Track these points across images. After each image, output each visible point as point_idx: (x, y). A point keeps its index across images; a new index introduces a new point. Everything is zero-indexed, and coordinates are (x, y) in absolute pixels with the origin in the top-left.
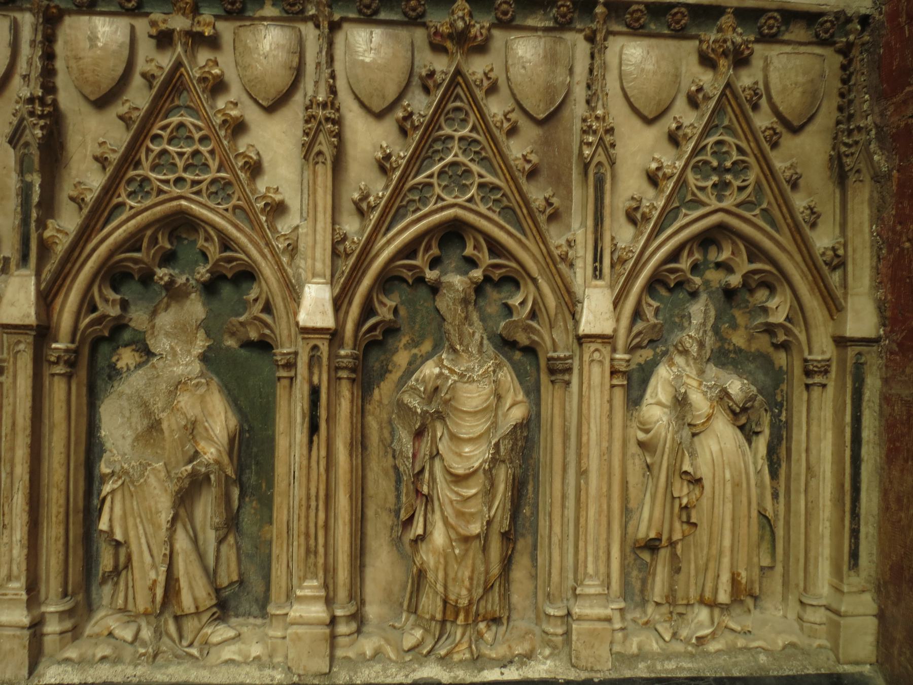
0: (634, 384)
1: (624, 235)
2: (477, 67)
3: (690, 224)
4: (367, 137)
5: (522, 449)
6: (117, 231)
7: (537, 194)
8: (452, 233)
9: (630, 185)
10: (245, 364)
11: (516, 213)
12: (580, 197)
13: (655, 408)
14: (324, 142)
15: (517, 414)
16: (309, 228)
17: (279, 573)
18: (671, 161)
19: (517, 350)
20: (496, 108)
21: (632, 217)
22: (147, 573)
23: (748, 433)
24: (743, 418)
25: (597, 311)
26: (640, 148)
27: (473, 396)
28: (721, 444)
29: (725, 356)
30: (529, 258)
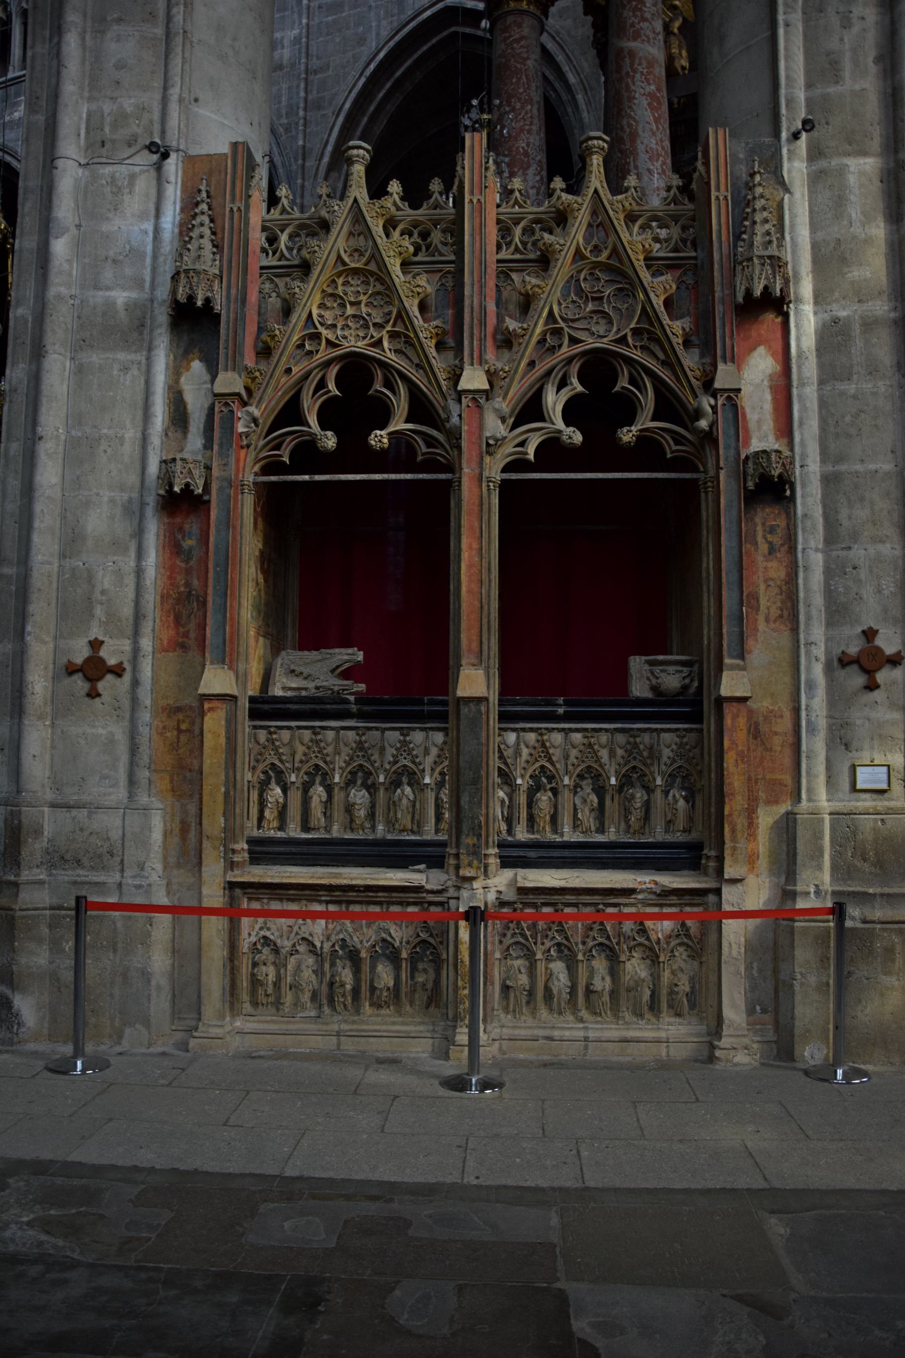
0: (666, 793)
1: (663, 767)
2: (638, 740)
3: (676, 765)
4: (620, 752)
5: (647, 805)
6: (580, 769)
7: (649, 761)
8: (634, 767)
9: (664, 759)
10: (600, 791)
11: (645, 764)
12: (656, 762)
14: (612, 754)
16: (611, 769)
18: (671, 754)
20: (641, 747)
21: (665, 764)
24: (686, 799)
25: (659, 781)
26: (666, 753)
27: (638, 795)
28: (681, 803)
29: (683, 788)
30: (647, 772)
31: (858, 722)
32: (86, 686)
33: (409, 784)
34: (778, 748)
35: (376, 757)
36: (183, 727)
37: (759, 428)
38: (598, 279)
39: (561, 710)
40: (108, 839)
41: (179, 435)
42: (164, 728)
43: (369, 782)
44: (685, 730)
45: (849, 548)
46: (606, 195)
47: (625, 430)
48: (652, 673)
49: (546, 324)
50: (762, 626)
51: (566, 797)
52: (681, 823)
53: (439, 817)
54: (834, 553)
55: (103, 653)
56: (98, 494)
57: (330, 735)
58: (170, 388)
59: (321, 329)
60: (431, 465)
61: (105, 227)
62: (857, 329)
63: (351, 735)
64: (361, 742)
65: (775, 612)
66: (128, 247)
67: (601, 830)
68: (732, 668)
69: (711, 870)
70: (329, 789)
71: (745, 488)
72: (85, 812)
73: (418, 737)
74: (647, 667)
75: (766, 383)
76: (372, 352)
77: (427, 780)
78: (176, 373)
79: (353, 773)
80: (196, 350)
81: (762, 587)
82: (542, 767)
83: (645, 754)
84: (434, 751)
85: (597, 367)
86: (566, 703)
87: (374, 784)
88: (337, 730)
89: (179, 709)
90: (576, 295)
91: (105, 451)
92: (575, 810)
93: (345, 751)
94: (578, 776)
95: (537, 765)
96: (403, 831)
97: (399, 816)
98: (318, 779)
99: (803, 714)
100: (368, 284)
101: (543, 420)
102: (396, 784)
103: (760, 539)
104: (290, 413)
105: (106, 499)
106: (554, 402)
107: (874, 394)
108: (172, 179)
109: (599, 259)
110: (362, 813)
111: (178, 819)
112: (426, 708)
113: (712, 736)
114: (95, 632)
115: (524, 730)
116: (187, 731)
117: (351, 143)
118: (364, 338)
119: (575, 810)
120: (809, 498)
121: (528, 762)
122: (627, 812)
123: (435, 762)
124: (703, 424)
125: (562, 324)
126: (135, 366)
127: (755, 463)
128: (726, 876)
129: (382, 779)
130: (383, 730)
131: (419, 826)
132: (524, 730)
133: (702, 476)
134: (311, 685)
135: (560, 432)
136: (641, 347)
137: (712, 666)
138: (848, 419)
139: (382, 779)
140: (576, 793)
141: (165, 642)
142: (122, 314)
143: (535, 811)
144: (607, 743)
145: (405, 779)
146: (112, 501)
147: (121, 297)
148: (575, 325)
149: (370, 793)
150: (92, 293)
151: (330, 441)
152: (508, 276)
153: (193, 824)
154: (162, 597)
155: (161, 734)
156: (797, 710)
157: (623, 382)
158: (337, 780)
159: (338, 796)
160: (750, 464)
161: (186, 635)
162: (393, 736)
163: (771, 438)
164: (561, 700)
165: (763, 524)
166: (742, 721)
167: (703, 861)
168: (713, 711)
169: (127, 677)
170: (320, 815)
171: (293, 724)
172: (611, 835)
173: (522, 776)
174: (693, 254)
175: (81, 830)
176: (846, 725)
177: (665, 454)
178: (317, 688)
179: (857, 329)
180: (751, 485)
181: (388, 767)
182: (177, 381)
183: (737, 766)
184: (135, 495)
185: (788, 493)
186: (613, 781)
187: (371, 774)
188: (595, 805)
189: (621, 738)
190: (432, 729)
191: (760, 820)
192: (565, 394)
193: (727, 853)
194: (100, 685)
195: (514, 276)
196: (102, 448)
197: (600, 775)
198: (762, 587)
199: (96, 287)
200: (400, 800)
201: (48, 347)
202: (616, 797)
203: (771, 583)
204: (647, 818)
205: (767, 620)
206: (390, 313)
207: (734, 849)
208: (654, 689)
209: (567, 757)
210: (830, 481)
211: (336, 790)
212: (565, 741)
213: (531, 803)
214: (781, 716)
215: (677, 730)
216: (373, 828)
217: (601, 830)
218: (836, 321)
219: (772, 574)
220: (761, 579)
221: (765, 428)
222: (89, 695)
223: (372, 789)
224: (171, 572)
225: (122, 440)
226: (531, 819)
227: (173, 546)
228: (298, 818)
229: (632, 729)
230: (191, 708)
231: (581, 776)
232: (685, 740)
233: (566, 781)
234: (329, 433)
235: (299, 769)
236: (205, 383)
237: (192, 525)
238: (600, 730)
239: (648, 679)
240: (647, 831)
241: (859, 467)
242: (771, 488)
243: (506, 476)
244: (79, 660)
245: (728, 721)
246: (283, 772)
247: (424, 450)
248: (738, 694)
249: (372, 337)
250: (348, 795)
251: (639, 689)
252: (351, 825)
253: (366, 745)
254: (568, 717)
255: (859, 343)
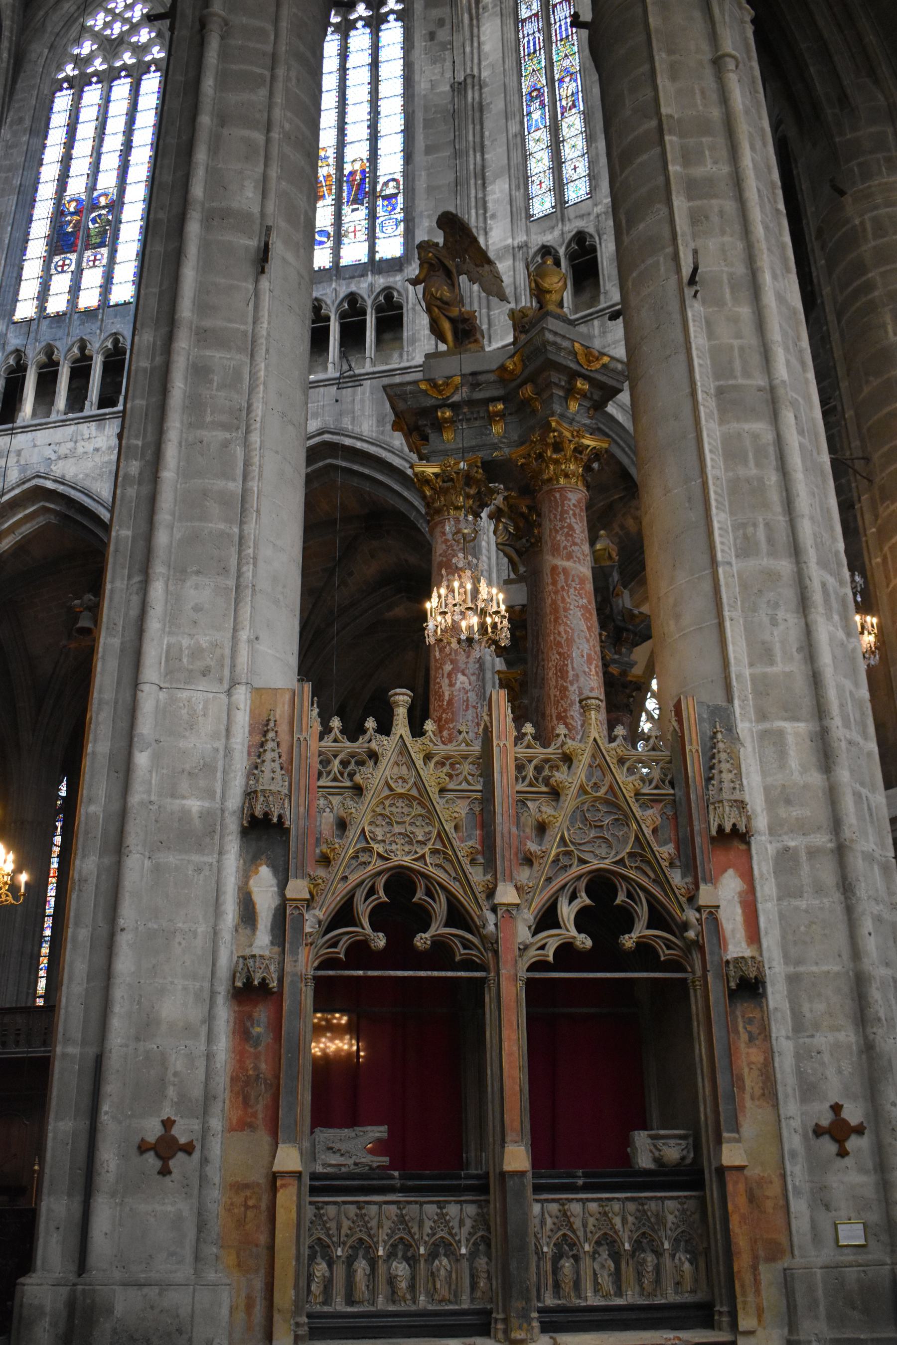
0: (673, 1256)
2: (646, 1207)
3: (680, 1230)
4: (631, 1219)
5: (658, 1269)
8: (644, 1233)
9: (669, 1225)
10: (616, 1256)
11: (653, 1230)
13: (677, 1261)
14: (624, 1221)
15: (656, 1261)
16: (625, 1236)
17: (624, 1288)
18: (675, 1220)
19: (655, 1252)
22: (605, 1288)
23: (691, 1263)
25: (666, 1246)
27: (649, 1259)
28: (687, 1266)
29: (687, 1251)
31: (835, 1185)
32: (158, 1164)
33: (446, 1255)
34: (771, 1211)
35: (415, 1229)
36: (251, 1203)
37: (734, 937)
38: (599, 810)
39: (580, 1182)
40: (178, 1316)
41: (248, 931)
42: (232, 1204)
43: (409, 1254)
44: (685, 1197)
45: (812, 1036)
46: (603, 744)
47: (627, 936)
48: (655, 1146)
49: (558, 847)
50: (748, 1103)
51: (586, 1264)
52: (688, 1284)
53: (474, 1286)
54: (801, 1041)
55: (175, 1131)
56: (172, 983)
57: (374, 1209)
58: (240, 889)
59: (373, 844)
60: (468, 964)
61: (182, 744)
62: (803, 857)
63: (393, 1209)
64: (403, 1216)
65: (758, 1092)
66: (202, 762)
67: (619, 1293)
68: (730, 1141)
69: (725, 1325)
70: (373, 1262)
71: (728, 987)
72: (156, 1290)
73: (453, 1210)
74: (649, 1141)
75: (736, 898)
76: (417, 866)
77: (463, 1251)
78: (246, 875)
79: (394, 1246)
80: (263, 857)
81: (746, 1070)
82: (564, 1235)
83: (653, 1220)
84: (468, 1223)
85: (601, 885)
86: (585, 1175)
87: (413, 1256)
88: (380, 1204)
89: (247, 1186)
90: (582, 822)
91: (180, 944)
92: (595, 1274)
93: (387, 1224)
94: (596, 1242)
95: (560, 1233)
96: (440, 1301)
97: (438, 1286)
98: (361, 1253)
99: (789, 1179)
100: (412, 807)
101: (559, 927)
102: (433, 1255)
103: (741, 1029)
104: (344, 915)
105: (180, 987)
106: (567, 912)
107: (822, 909)
108: (242, 706)
109: (598, 794)
110: (403, 1285)
111: (243, 1295)
112: (463, 1182)
113: (716, 1201)
114: (167, 1112)
115: (547, 1201)
116: (253, 1207)
117: (398, 690)
118: (409, 853)
119: (595, 1274)
120: (776, 995)
121: (552, 1230)
122: (640, 1275)
123: (470, 1234)
124: (691, 934)
125: (572, 848)
126: (207, 868)
127: (735, 967)
128: (741, 1329)
129: (422, 1250)
130: (421, 1204)
131: (456, 1296)
132: (547, 1201)
133: (689, 976)
134: (350, 1162)
135: (574, 938)
136: (636, 867)
137: (711, 1139)
138: (802, 928)
139: (422, 1250)
140: (594, 1259)
141: (234, 1121)
142: (197, 821)
143: (560, 1278)
144: (619, 1211)
145: (442, 1250)
146: (185, 989)
147: (195, 805)
148: (582, 848)
149: (409, 1265)
150: (169, 800)
151: (380, 941)
152: (524, 804)
153: (258, 1300)
154: (232, 1079)
155: (229, 1210)
156: (784, 1176)
157: (621, 898)
158: (381, 1253)
159: (382, 1268)
160: (731, 967)
161: (254, 1115)
162: (431, 1210)
163: (744, 945)
164: (580, 1173)
165: (743, 1017)
166: (741, 1187)
167: (716, 1317)
168: (714, 1179)
169: (196, 1155)
170: (364, 1288)
171: (339, 1199)
172: (631, 1297)
173: (548, 1244)
174: (672, 792)
175: (152, 1308)
176: (823, 1188)
177: (659, 957)
178: (356, 1164)
179: (803, 857)
180: (733, 985)
181: (427, 1239)
182: (246, 883)
183: (741, 1227)
184: (207, 985)
185: (761, 990)
186: (627, 1246)
187: (411, 1246)
188: (612, 1269)
189: (631, 1207)
190: (466, 1202)
191: (762, 1277)
192: (577, 905)
193: (739, 1306)
194: (171, 1163)
195: (529, 804)
196: (177, 940)
197: (615, 1241)
198: (746, 1070)
199: (173, 796)
200: (438, 1270)
201: (132, 848)
202: (631, 1262)
203: (753, 1066)
204: (658, 1281)
205: (752, 1098)
206: (430, 833)
207: (745, 1303)
208: (656, 1160)
209: (585, 1226)
210: (793, 980)
211: (380, 1262)
212: (584, 1209)
213: (556, 1270)
214: (771, 1182)
215: (678, 1197)
216: (414, 1300)
217: (619, 1293)
218: (787, 849)
219: (753, 1058)
220: (745, 1064)
221: (738, 936)
222: (159, 1173)
223: (412, 1261)
224: (240, 1055)
225: (195, 934)
226: (557, 1286)
227: (242, 1032)
228: (343, 1292)
229: (641, 1198)
230: (258, 1184)
231: (598, 1243)
232: (685, 1206)
233: (587, 1247)
234: (381, 935)
235: (344, 1243)
236: (272, 886)
237: (262, 1014)
238: (613, 1199)
239: (651, 1151)
240: (658, 1293)
241: (814, 969)
242: (749, 987)
243: (530, 975)
244: (151, 1139)
245: (730, 1187)
246: (329, 1247)
247: (463, 951)
248: (737, 1163)
249: (416, 852)
250: (389, 1268)
251: (644, 1161)
252: (393, 1295)
253: (407, 1218)
254: (586, 1188)
255: (805, 868)
